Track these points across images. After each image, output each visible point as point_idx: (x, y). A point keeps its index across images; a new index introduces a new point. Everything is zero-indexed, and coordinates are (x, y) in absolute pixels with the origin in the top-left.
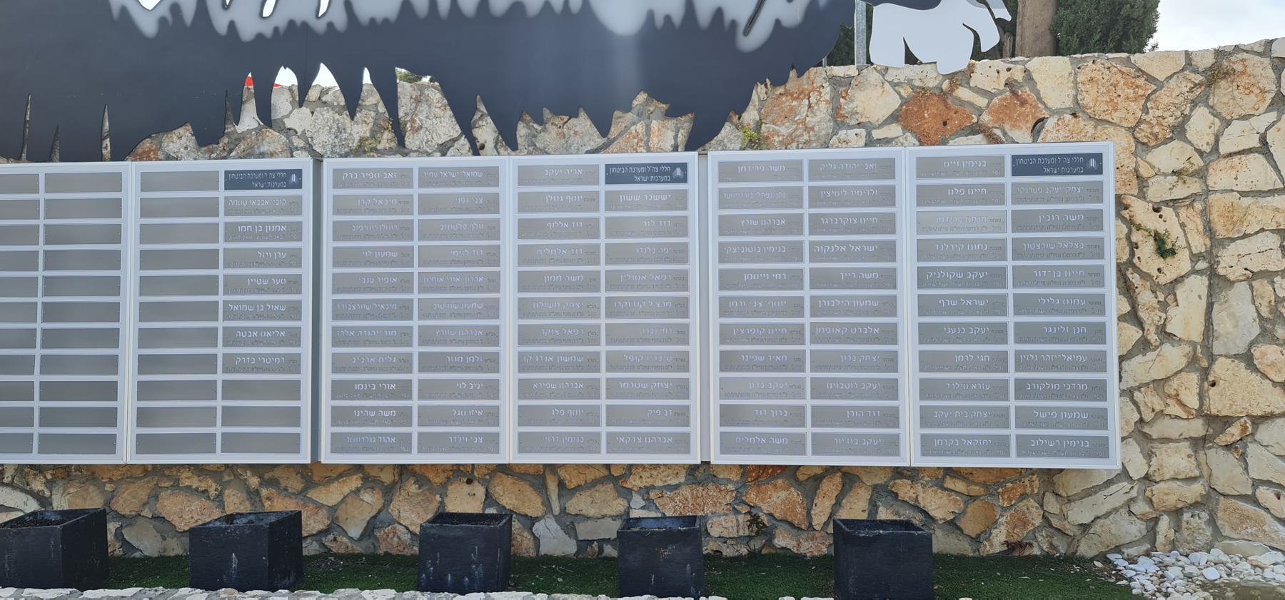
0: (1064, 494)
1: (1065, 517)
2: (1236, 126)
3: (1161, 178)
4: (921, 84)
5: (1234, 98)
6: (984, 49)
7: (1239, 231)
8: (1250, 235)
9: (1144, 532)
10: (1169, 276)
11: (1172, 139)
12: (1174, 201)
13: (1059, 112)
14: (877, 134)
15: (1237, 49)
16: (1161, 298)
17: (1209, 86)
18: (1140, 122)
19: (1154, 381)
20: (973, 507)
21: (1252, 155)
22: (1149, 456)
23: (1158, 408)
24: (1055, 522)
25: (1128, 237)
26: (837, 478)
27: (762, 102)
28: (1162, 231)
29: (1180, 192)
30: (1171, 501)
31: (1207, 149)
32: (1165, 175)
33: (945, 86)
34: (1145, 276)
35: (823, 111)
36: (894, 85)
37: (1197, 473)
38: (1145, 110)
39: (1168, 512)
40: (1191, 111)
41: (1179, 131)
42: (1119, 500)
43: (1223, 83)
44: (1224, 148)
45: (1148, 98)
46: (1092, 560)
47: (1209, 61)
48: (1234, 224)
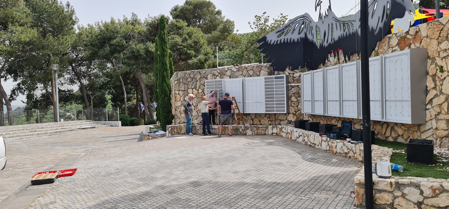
10: (443, 77)
13: (424, 37)
14: (394, 49)
16: (441, 83)
18: (439, 36)
20: (406, 132)
22: (437, 123)
23: (438, 111)
25: (436, 67)
26: (386, 124)
27: (379, 45)
30: (440, 135)
34: (439, 77)
35: (387, 46)
36: (397, 37)
37: (447, 129)
38: (440, 33)
39: (440, 138)
42: (430, 134)
45: (442, 30)
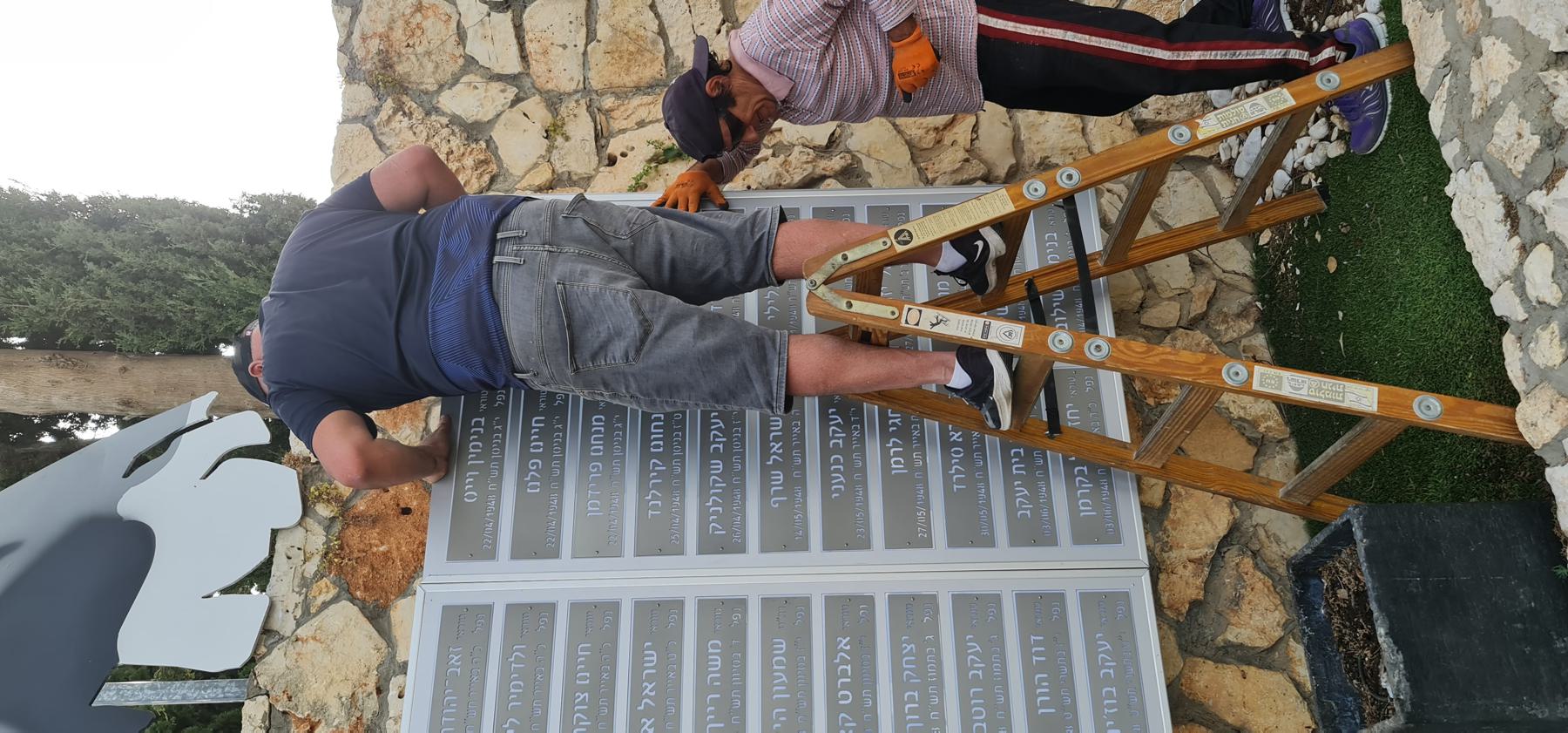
0: (1140, 294)
1: (1184, 294)
2: (475, 48)
3: (555, 155)
4: (316, 560)
5: (428, 53)
6: (263, 436)
7: (654, 43)
8: (661, 25)
9: (1187, 174)
11: (489, 141)
12: (598, 136)
15: (344, 48)
17: (405, 91)
19: (914, 160)
21: (527, 24)
24: (1198, 307)
28: (650, 151)
29: (581, 128)
31: (512, 92)
32: (550, 149)
33: (324, 511)
36: (306, 615)
40: (444, 114)
41: (474, 131)
43: (400, 69)
44: (513, 66)
46: (1258, 250)
47: (364, 93)
48: (640, 51)
